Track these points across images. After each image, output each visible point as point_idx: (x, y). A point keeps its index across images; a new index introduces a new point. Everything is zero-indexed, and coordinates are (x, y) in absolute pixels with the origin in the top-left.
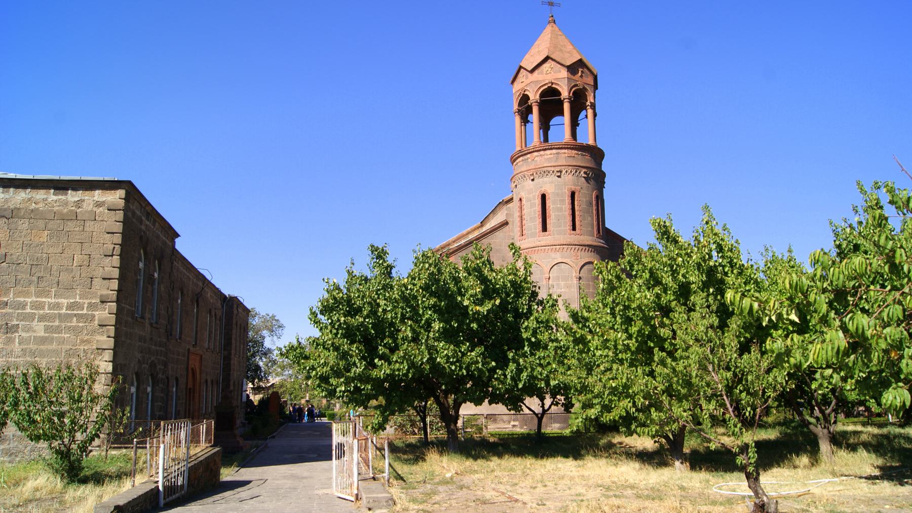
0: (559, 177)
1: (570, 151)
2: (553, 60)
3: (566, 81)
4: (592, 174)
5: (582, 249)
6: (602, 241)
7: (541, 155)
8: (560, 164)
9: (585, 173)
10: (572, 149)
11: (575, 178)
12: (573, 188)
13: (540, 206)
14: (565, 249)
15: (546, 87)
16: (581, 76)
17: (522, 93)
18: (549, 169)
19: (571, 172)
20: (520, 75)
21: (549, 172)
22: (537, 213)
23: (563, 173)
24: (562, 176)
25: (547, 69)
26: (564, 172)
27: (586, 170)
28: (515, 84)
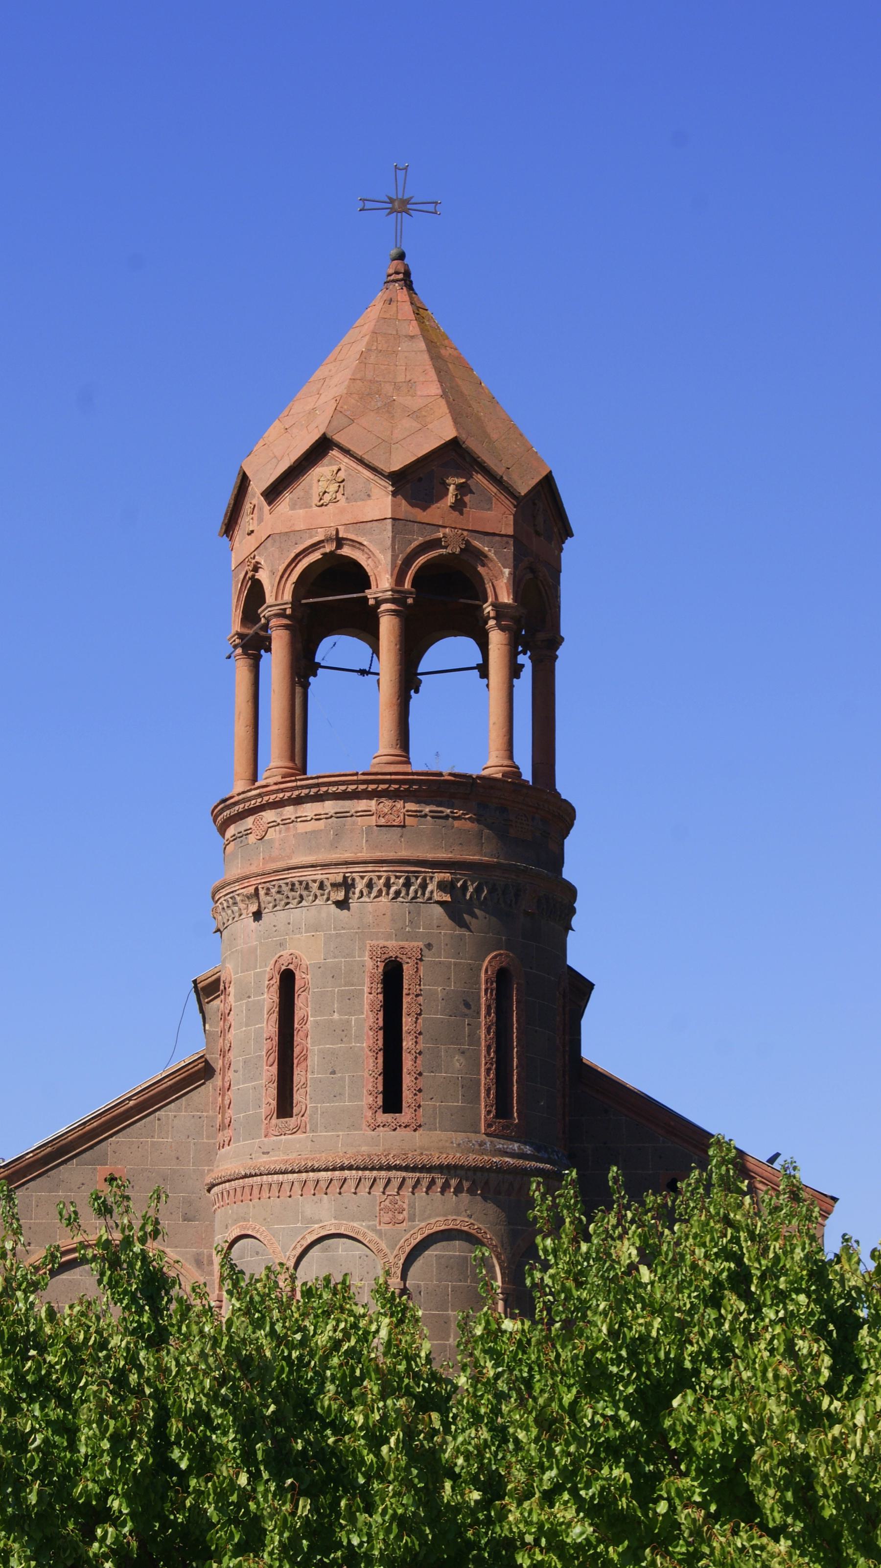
0: (342, 905)
1: (388, 803)
2: (346, 452)
3: (389, 527)
4: (478, 890)
5: (418, 1182)
6: (516, 1146)
7: (286, 822)
8: (348, 856)
9: (442, 886)
10: (395, 796)
11: (402, 906)
12: (393, 946)
13: (275, 1016)
14: (351, 1185)
15: (316, 556)
16: (459, 506)
17: (250, 574)
18: (309, 875)
19: (388, 885)
20: (247, 507)
21: (307, 888)
22: (266, 1045)
23: (357, 891)
24: (354, 904)
25: (323, 485)
26: (360, 885)
27: (447, 876)
28: (239, 534)
